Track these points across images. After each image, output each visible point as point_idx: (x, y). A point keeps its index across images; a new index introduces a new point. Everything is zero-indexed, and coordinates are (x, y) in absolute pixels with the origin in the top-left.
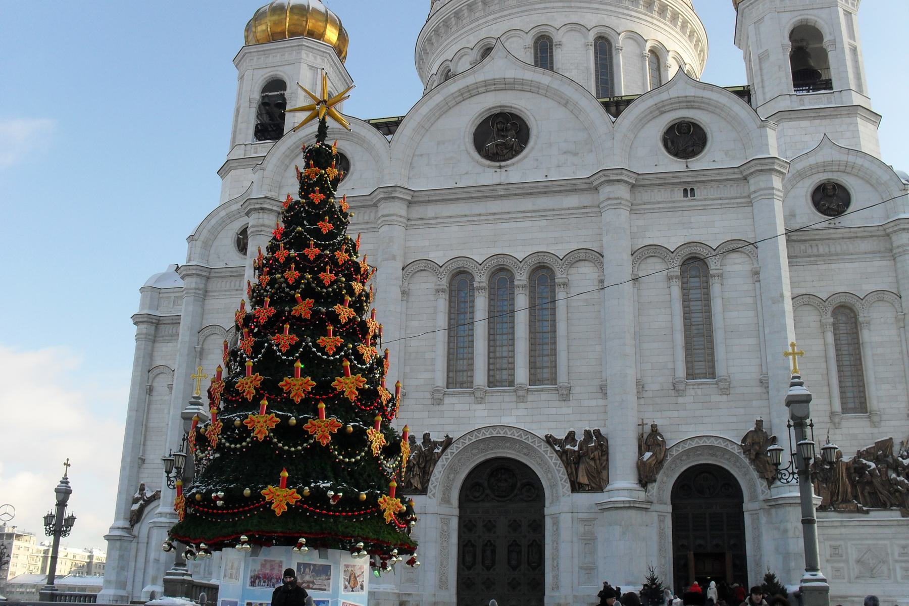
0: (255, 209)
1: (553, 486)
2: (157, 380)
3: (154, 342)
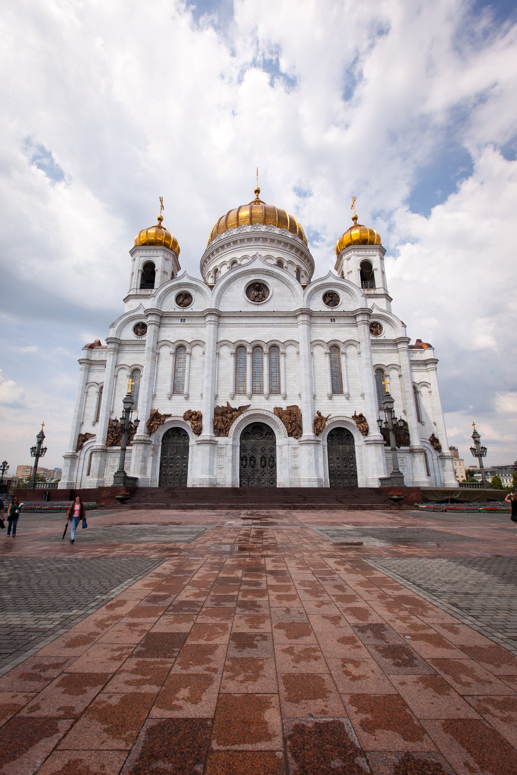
2: (90, 388)
3: (89, 371)
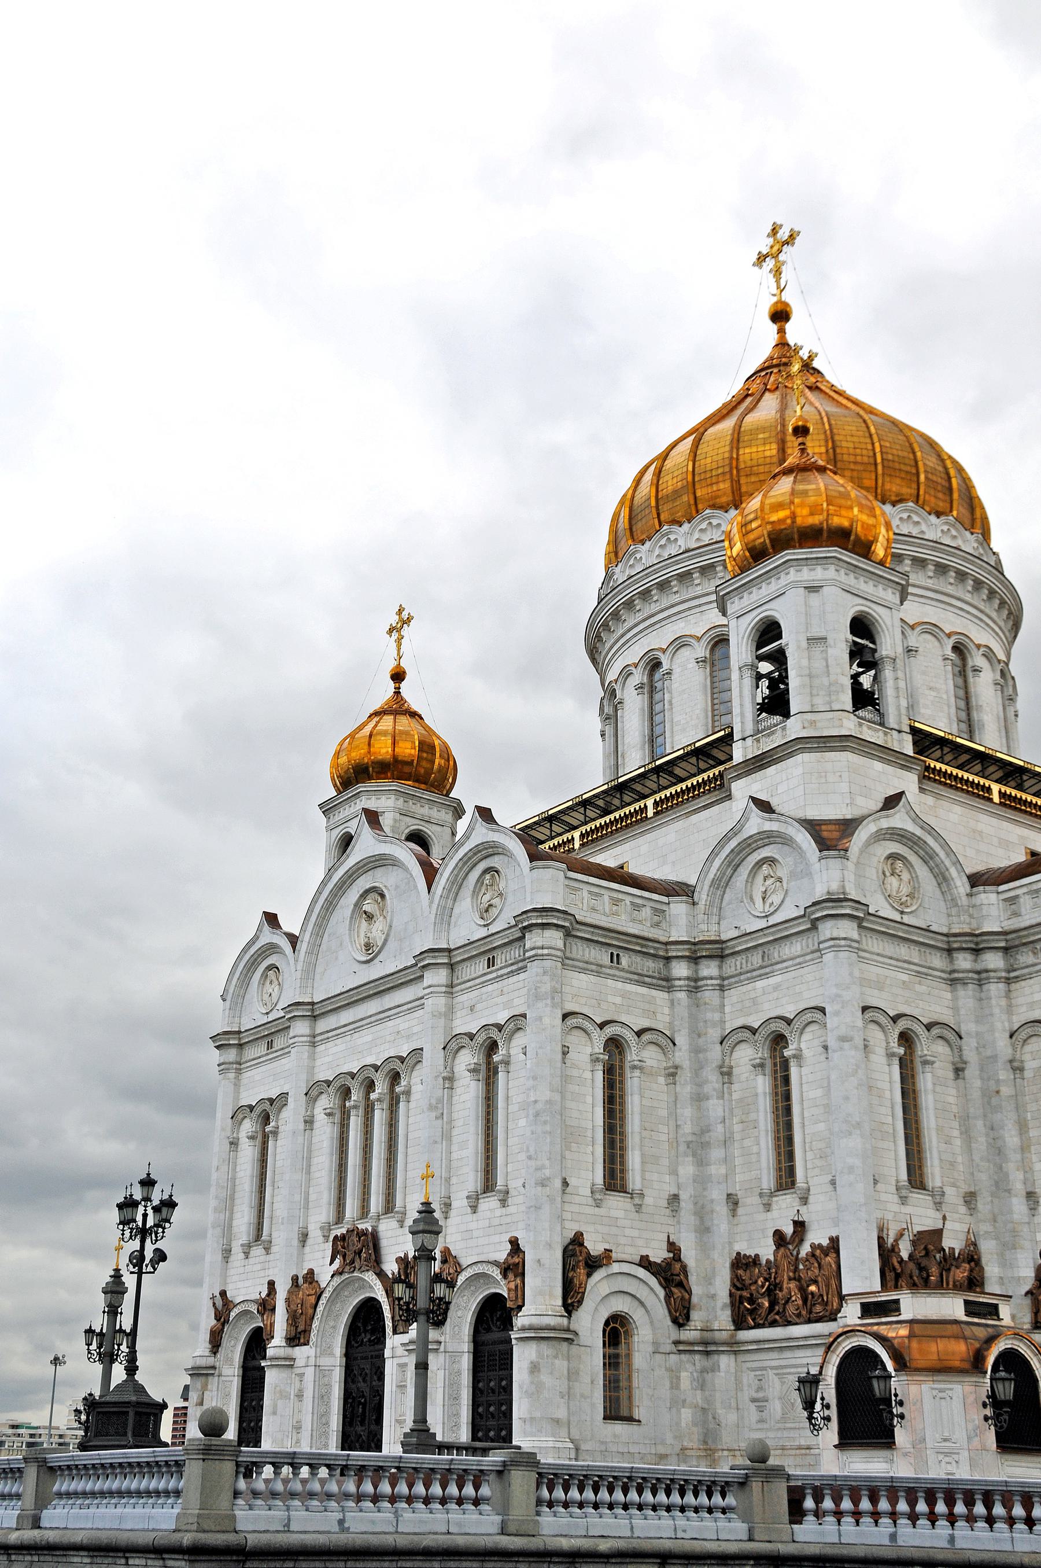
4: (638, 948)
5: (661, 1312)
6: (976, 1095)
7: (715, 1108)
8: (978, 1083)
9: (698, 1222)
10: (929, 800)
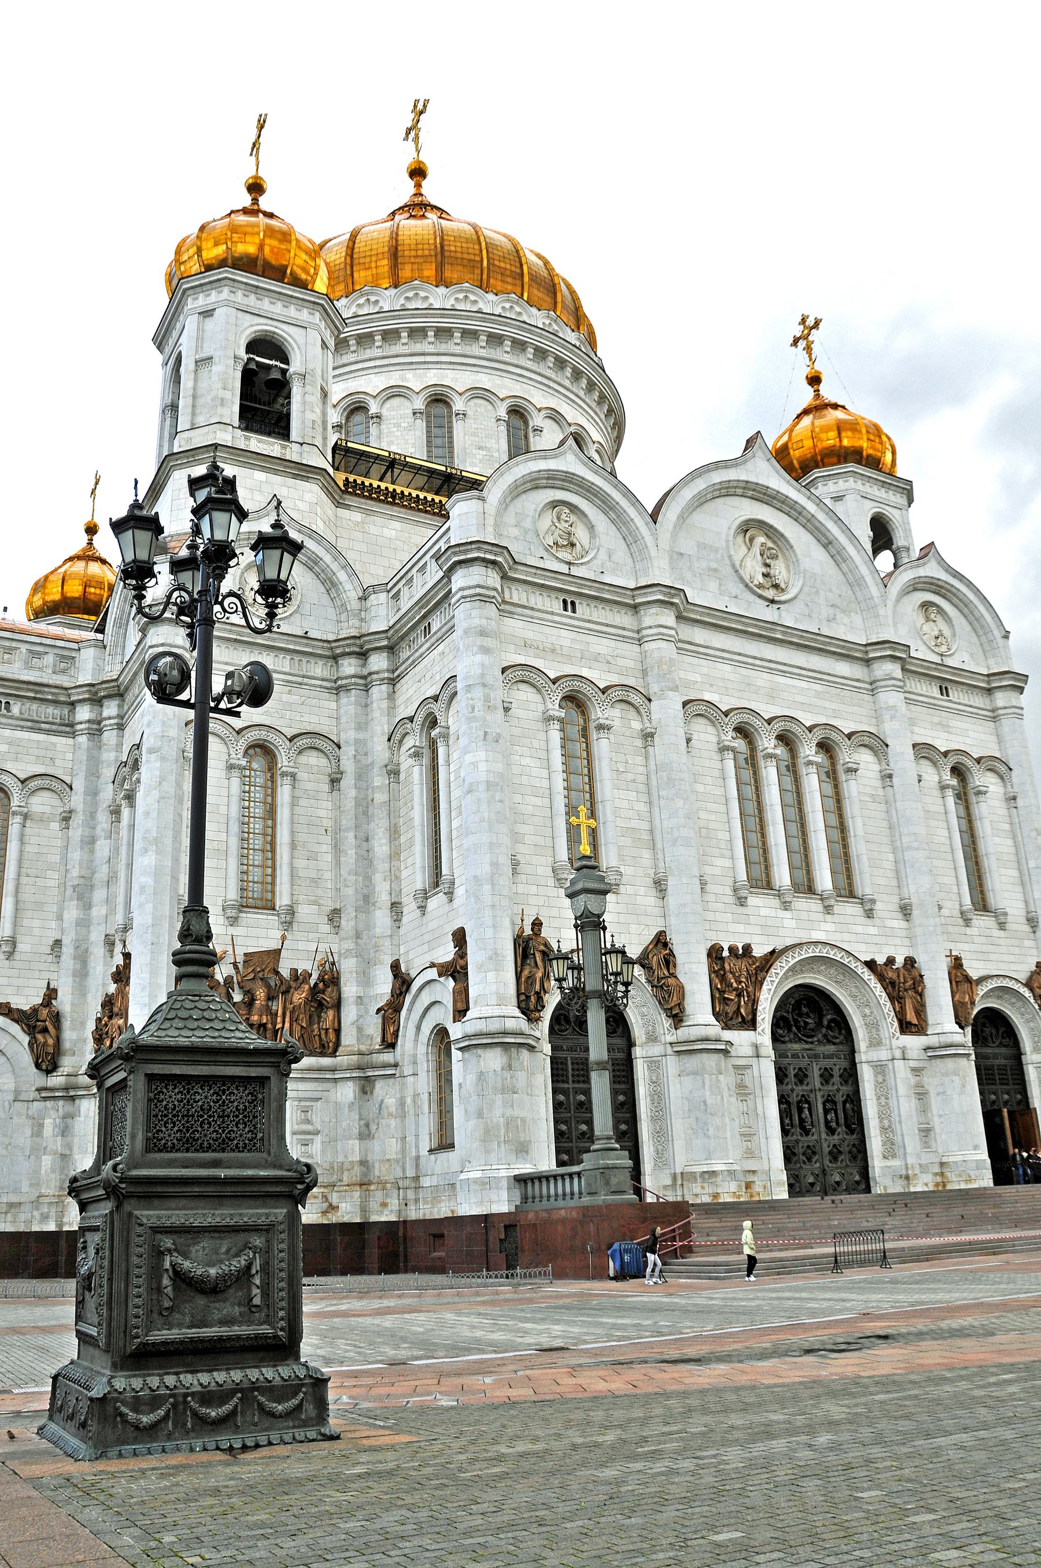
0: (484, 560)
1: (873, 1026)
4: (32, 695)
5: (26, 1059)
6: (349, 805)
7: (103, 848)
8: (353, 793)
9: (78, 967)
10: (357, 516)
